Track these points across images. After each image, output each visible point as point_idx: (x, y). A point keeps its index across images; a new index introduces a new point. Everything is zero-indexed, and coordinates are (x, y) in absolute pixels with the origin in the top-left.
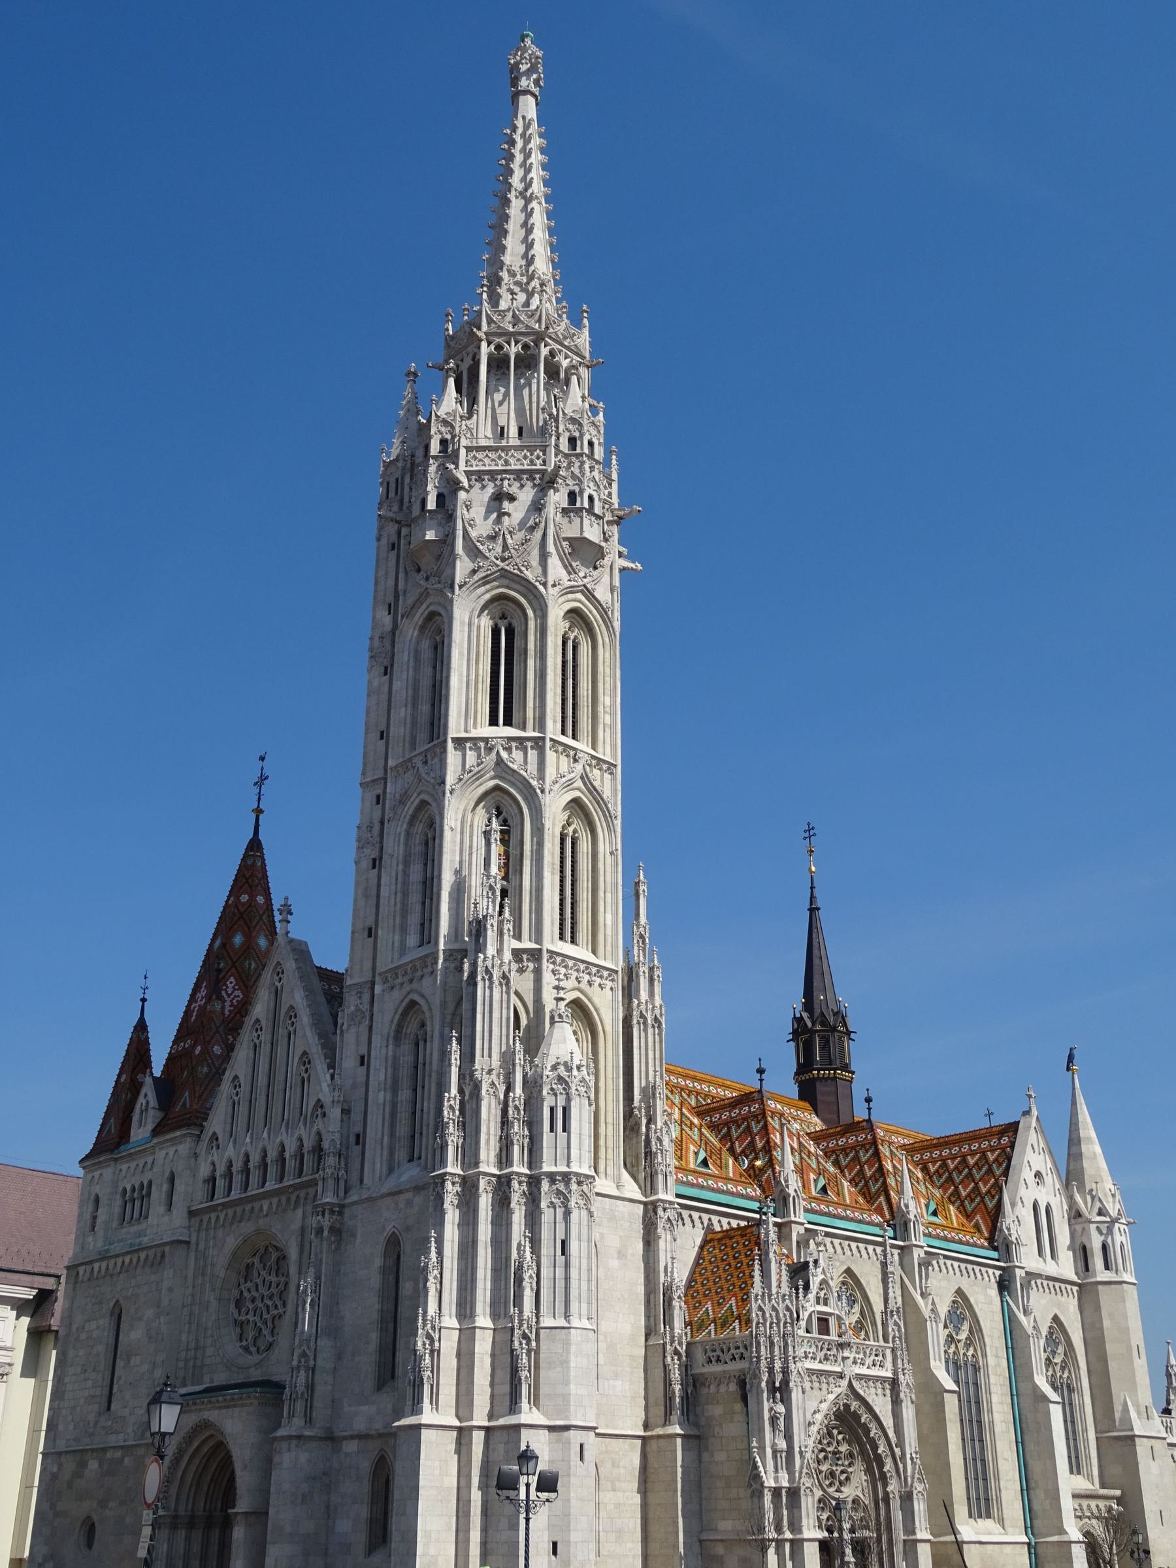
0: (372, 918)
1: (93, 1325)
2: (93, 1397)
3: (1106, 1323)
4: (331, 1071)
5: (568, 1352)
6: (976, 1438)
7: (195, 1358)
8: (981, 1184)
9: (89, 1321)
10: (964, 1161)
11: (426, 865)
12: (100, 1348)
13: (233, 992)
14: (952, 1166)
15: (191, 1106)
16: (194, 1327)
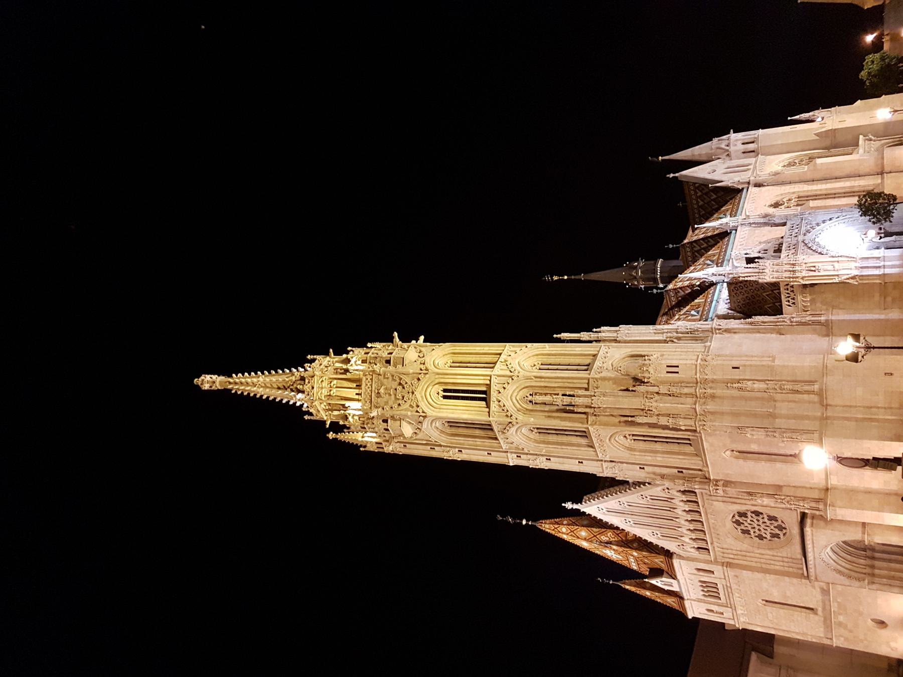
0: (574, 461)
1: (770, 615)
2: (806, 617)
3: (779, 142)
4: (647, 484)
5: (788, 366)
6: (834, 196)
7: (788, 562)
8: (712, 198)
9: (768, 618)
10: (701, 207)
11: (549, 433)
12: (782, 611)
13: (608, 537)
14: (704, 212)
15: (662, 558)
16: (772, 562)
